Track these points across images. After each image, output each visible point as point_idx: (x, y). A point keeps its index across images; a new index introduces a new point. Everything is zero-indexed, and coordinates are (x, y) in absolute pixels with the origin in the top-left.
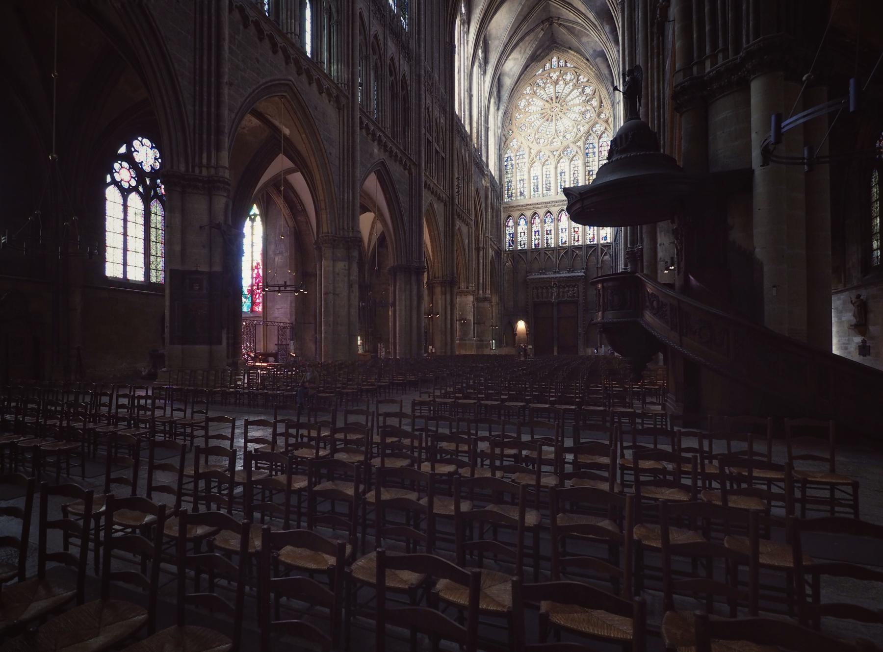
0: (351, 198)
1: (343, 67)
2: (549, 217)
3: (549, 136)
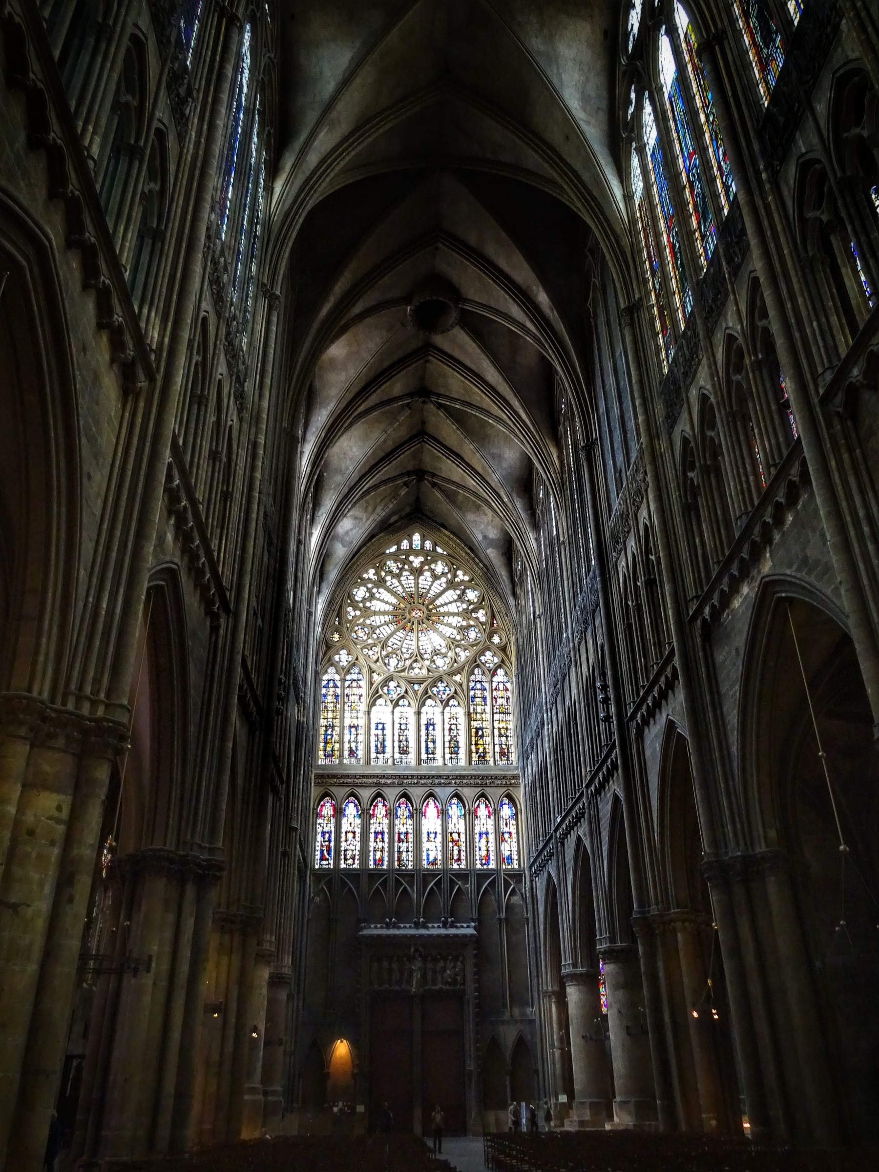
0: (118, 610)
1: (153, 314)
2: (403, 806)
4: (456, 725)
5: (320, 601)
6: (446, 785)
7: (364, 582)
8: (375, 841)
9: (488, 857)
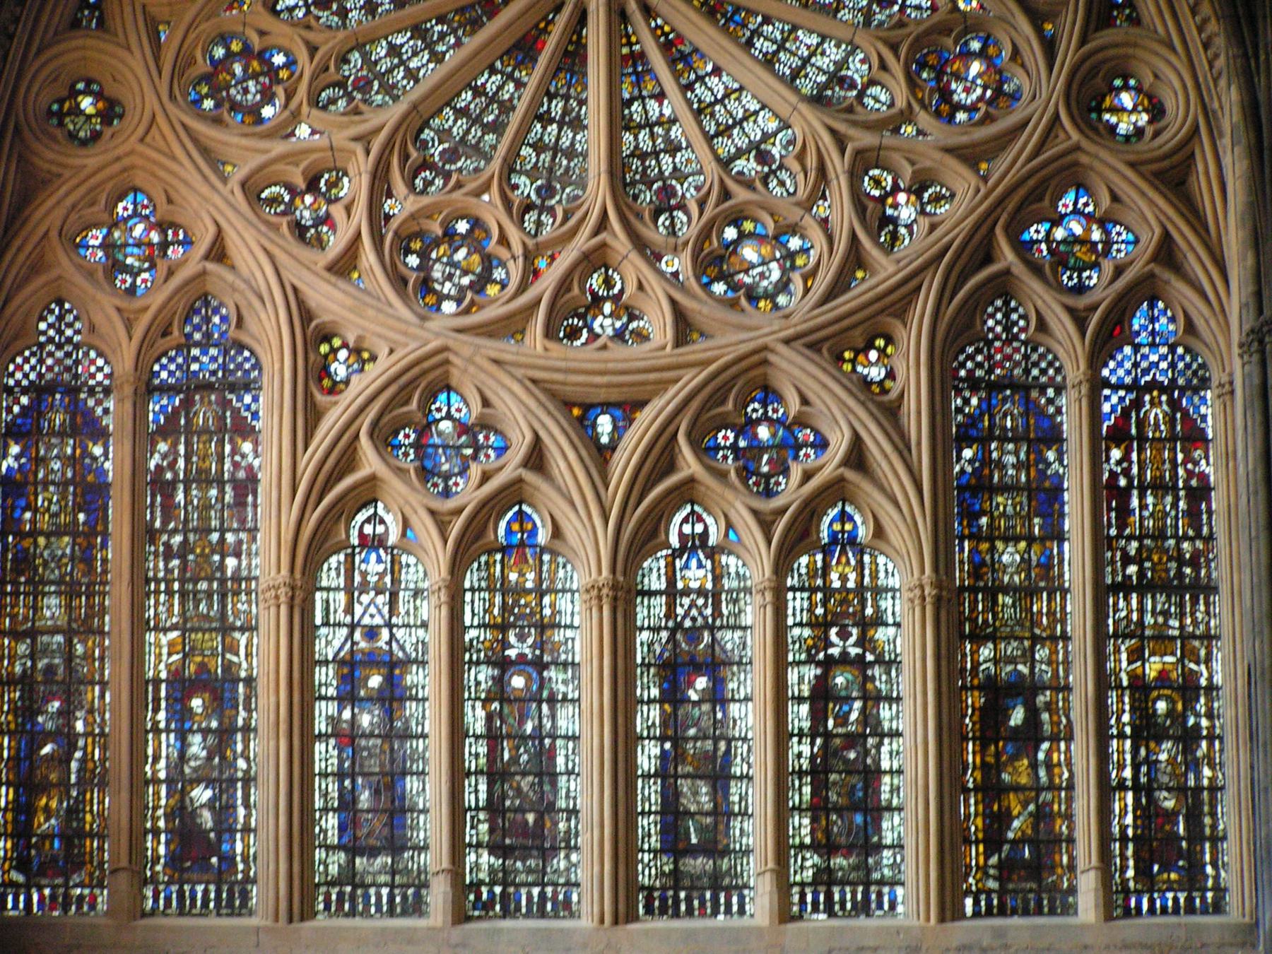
4: (860, 662)
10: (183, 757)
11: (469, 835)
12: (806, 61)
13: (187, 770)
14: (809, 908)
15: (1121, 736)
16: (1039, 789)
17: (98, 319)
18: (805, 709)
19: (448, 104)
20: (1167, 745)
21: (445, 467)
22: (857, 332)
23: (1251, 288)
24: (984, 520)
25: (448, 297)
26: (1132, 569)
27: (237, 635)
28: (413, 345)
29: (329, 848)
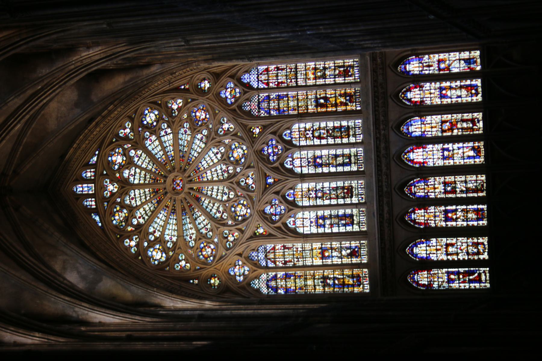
3: (232, 194)
4: (313, 131)
5: (172, 304)
6: (387, 142)
7: (141, 251)
8: (456, 220)
9: (469, 88)
10: (336, 257)
11: (349, 202)
12: (198, 146)
13: (339, 255)
14: (360, 138)
15: (325, 81)
16: (335, 97)
17: (254, 277)
18: (322, 141)
19: (209, 213)
20: (326, 72)
21: (279, 210)
22: (250, 134)
23: (240, 60)
24: (285, 109)
25: (247, 211)
26: (293, 81)
27: (313, 247)
28: (256, 217)
29: (353, 228)
